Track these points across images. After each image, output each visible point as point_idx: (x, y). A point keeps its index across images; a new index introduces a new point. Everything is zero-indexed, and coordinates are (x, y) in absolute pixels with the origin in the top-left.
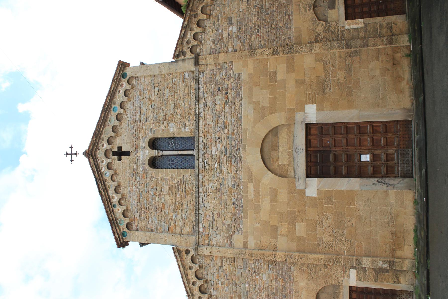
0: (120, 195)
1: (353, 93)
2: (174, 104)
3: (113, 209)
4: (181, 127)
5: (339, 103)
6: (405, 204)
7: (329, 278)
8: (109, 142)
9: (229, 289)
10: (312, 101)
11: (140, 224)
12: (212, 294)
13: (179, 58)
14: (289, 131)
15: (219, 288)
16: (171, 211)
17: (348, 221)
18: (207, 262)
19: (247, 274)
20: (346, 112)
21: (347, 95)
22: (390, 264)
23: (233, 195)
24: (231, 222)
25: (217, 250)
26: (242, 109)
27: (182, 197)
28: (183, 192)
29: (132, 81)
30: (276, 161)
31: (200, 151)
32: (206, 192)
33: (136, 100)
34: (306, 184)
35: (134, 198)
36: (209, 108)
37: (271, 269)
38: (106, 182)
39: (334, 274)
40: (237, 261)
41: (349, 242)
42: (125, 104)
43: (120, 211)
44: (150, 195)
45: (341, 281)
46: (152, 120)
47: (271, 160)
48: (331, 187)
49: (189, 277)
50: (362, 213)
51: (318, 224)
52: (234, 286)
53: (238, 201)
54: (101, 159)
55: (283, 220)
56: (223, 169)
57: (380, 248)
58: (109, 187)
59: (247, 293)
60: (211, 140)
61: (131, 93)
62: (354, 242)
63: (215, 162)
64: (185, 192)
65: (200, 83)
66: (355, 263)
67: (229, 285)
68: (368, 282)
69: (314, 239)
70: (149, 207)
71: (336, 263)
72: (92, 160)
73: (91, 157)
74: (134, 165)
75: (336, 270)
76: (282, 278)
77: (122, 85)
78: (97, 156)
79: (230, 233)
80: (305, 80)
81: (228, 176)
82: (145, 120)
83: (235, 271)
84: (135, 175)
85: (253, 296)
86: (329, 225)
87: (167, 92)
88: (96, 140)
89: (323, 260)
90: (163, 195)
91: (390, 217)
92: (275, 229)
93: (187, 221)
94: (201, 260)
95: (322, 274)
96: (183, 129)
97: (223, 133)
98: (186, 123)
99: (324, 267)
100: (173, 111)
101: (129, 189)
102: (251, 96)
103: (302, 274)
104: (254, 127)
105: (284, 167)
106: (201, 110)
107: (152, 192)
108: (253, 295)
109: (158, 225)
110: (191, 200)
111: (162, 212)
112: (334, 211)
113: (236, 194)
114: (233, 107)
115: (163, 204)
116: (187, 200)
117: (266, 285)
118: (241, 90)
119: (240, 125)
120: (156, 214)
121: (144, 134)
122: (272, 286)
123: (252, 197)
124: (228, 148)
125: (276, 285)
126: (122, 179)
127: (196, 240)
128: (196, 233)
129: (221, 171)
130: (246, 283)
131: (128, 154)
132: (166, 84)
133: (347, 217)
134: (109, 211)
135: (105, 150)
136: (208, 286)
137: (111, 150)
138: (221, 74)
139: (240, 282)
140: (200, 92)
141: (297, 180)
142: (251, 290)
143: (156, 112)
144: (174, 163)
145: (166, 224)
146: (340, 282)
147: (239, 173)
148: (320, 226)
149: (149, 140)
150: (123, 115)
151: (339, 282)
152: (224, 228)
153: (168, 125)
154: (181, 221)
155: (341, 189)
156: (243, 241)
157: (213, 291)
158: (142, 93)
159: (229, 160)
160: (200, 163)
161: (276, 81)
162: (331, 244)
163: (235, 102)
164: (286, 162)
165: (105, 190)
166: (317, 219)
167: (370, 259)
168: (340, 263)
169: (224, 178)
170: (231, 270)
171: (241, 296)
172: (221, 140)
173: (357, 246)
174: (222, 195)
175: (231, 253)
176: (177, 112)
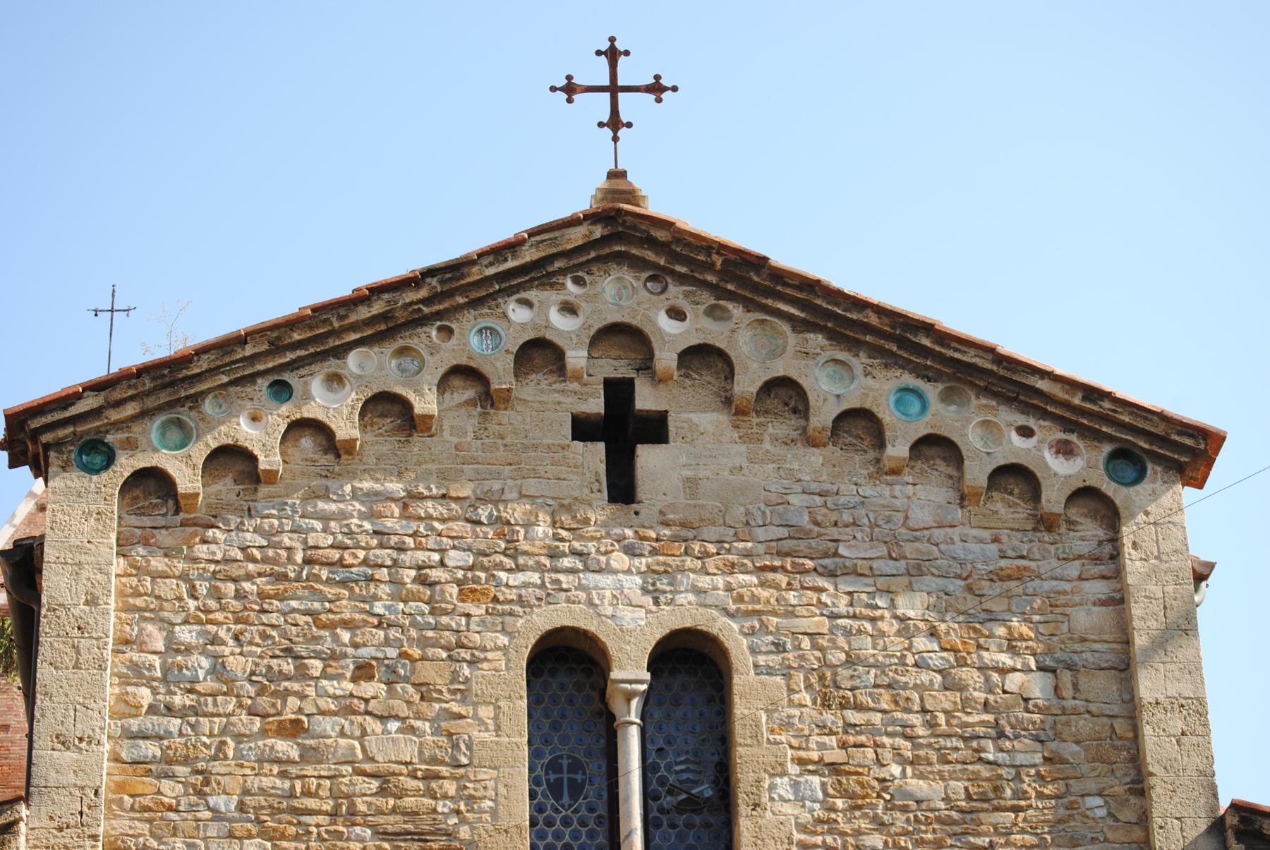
0: (356, 433)
3: (260, 381)
13: (1239, 841)
29: (1092, 515)
38: (434, 333)
42: (942, 466)
54: (589, 299)
58: (403, 352)
72: (576, 236)
73: (598, 232)
77: (1065, 450)
78: (607, 272)
87: (1020, 759)
88: (713, 264)
126: (455, 440)
134: (249, 351)
135: (647, 330)
137: (646, 365)
144: (566, 799)
149: (715, 631)
165: (383, 327)
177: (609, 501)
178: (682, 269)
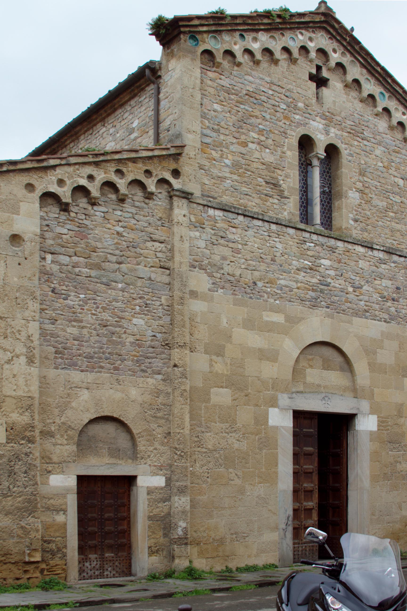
4: (355, 213)
5: (377, 463)
6: (262, 555)
7: (148, 441)
10: (381, 426)
12: (95, 208)
15: (109, 226)
18: (156, 210)
19: (142, 289)
20: (368, 472)
23: (267, 285)
26: (375, 320)
27: (258, 187)
28: (265, 191)
30: (309, 364)
31: (326, 239)
33: (388, 138)
34: (283, 409)
37: (154, 336)
40: (164, 272)
41: (206, 474)
45: (145, 462)
50: (248, 494)
51: (230, 426)
52: (118, 259)
53: (259, 292)
55: (234, 368)
56: (303, 274)
62: (207, 482)
64: (266, 195)
66: (181, 484)
67: (117, 249)
70: (239, 113)
71: (178, 453)
76: (141, 356)
79: (209, 267)
80: (402, 417)
82: (364, 148)
83: (145, 266)
86: (230, 442)
89: (182, 431)
90: (261, 149)
91: (244, 535)
92: (220, 353)
94: (160, 199)
95: (153, 428)
96: (351, 215)
99: (165, 433)
103: (149, 394)
105: (302, 376)
106: (376, 253)
107: (264, 128)
110: (254, 204)
111: (231, 137)
113: (269, 290)
114: (377, 307)
115: (245, 144)
116: (254, 195)
119: (356, 314)
120: (229, 123)
122: (124, 336)
123: (266, 318)
124: (329, 288)
125: (127, 344)
130: (123, 284)
133: (243, 472)
136: (111, 202)
139: (126, 272)
141: (290, 396)
142: (114, 293)
143: (373, 173)
148: (227, 429)
149: (338, 146)
150: (371, 108)
151: (142, 458)
152: (217, 258)
154: (220, 175)
156: (200, 290)
158: (397, 154)
159: (315, 288)
161: (404, 376)
163: (383, 311)
164: (309, 379)
166: (238, 425)
167: (188, 508)
168: (179, 459)
169: (290, 273)
170: (146, 257)
171: (99, 268)
174: (266, 265)
175: (181, 263)
176: (373, 211)
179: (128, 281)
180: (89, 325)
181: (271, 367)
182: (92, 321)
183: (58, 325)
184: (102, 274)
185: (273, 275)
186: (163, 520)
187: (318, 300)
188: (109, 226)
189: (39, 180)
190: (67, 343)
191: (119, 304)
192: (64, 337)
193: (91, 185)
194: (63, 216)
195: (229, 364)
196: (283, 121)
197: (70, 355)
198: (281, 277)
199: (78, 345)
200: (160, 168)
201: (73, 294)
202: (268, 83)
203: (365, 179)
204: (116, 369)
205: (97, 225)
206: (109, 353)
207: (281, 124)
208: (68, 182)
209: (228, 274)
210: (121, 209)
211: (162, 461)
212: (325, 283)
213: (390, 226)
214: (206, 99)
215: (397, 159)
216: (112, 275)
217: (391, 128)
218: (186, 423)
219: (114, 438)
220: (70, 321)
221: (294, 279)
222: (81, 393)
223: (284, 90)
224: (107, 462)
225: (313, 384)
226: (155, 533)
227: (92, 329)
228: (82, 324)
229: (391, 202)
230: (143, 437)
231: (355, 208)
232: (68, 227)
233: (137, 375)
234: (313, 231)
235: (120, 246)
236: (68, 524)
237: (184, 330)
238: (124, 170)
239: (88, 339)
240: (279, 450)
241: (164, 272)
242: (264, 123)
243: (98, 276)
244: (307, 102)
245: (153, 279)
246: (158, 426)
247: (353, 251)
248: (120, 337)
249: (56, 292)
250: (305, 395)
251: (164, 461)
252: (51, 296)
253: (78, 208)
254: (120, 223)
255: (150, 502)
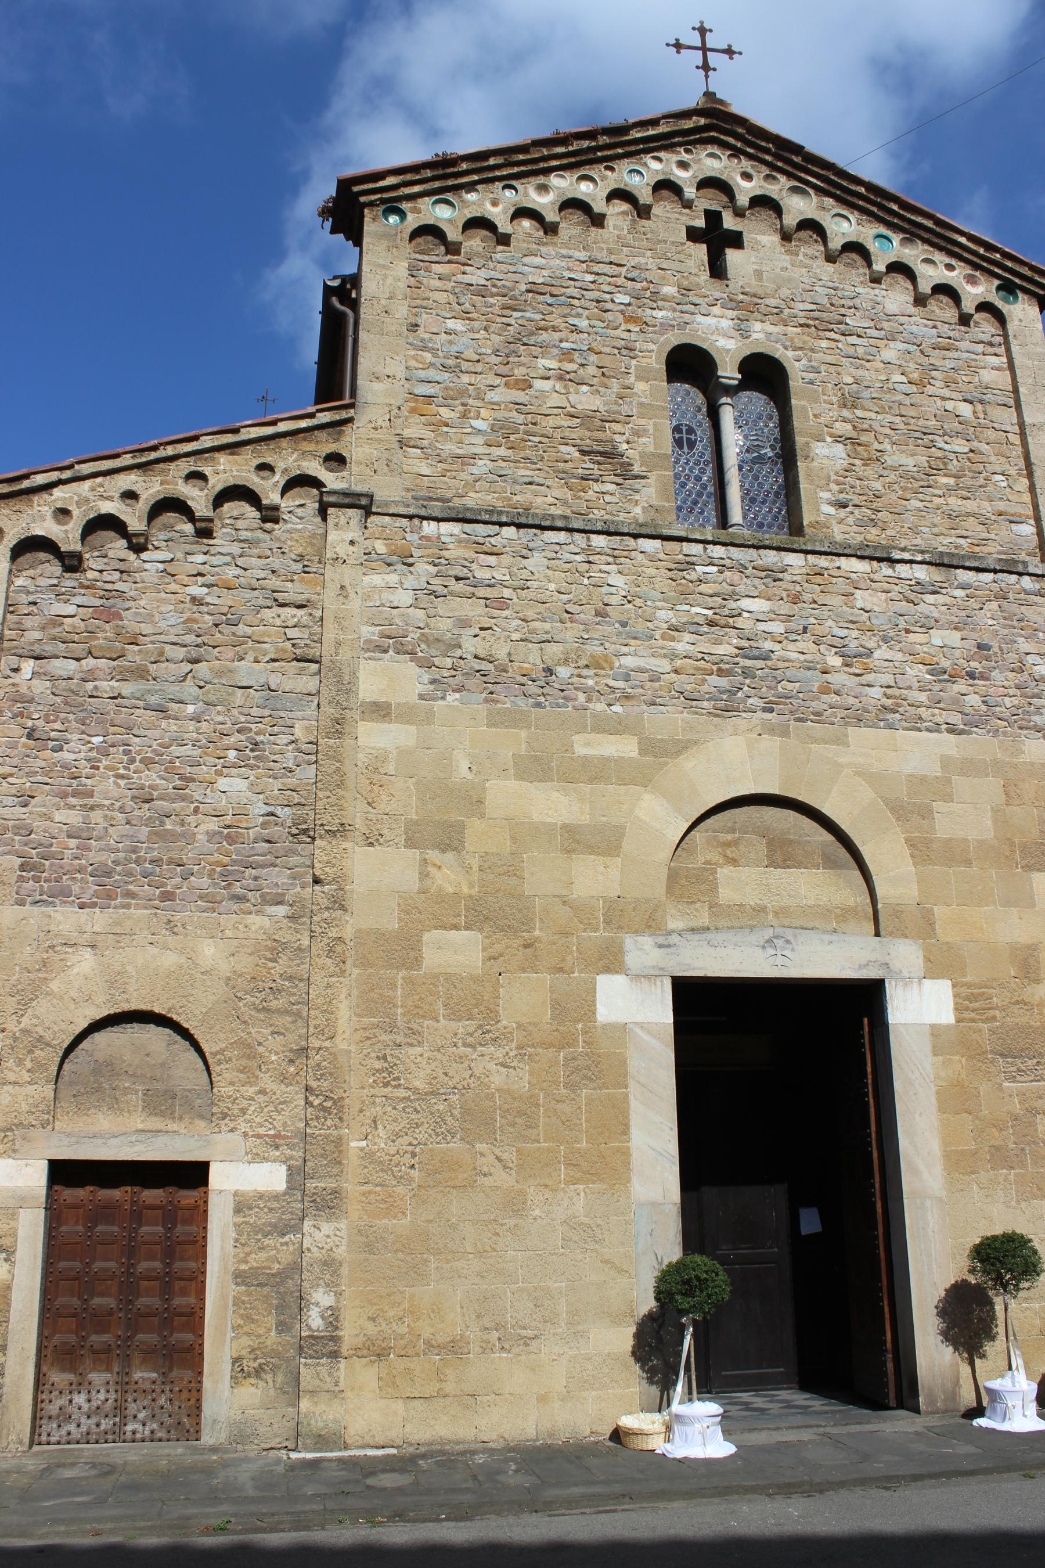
1: (1004, 1171)
2: (915, 469)
7: (241, 1071)
8: (762, 202)
9: (173, 630)
10: (967, 1009)
11: (437, 283)
12: (144, 556)
14: (845, 914)
16: (500, 415)
17: (499, 1154)
19: (246, 711)
20: (934, 1145)
21: (998, 1149)
22: (323, 1337)
23: (585, 672)
24: (469, 657)
25: (349, 587)
26: (919, 730)
27: (561, 465)
28: (580, 471)
30: (725, 856)
32: (589, 562)
33: (918, 325)
35: (545, 273)
36: (913, 602)
39: (260, 1092)
40: (303, 669)
41: (407, 1159)
43: (488, 206)
44: (563, 335)
46: (850, 380)
47: (729, 837)
48: (639, 1082)
49: (223, 460)
50: (537, 1212)
51: (480, 1026)
52: (189, 652)
53: (562, 691)
55: (491, 876)
56: (687, 637)
57: (389, 1295)
59: (159, 705)
60: (796, 599)
61: (943, 310)
62: (411, 1180)
63: (711, 608)
64: (583, 479)
65: (1000, 576)
66: (323, 1185)
67: (189, 631)
68: (232, 1243)
69: (416, 1007)
70: (509, 328)
71: (316, 1102)
73: (702, 121)
74: (676, 289)
75: (280, 1103)
76: (234, 862)
79: (423, 646)
81: (660, 656)
82: (851, 351)
84: (638, 286)
85: (142, 732)
86: (477, 1072)
87: (957, 449)
89: (327, 1044)
90: (565, 387)
91: (524, 1333)
93: (463, 476)
94: (301, 518)
95: (259, 1039)
96: (826, 495)
97: (827, 649)
98: (847, 509)
99: (291, 1050)
100: (889, 462)
101: (582, 255)
102: (969, 767)
104: (858, 773)
105: (703, 887)
106: (903, 570)
108: (146, 733)
109: (436, 356)
110: (550, 500)
112: (541, 1095)
113: (590, 682)
114: (923, 697)
116: (548, 482)
117: (195, 791)
118: (989, 732)
119: (858, 718)
120: (483, 350)
121: (796, 340)
122: (192, 819)
123: (580, 750)
124: (769, 663)
125: (199, 837)
127: (387, 504)
128: (417, 507)
129: (677, 630)
131: (717, 270)
132: (984, 447)
133: (518, 1150)
135: (731, 183)
136: (182, 540)
138: (1037, 657)
140: (971, 574)
141: (661, 940)
143: (880, 399)
144: (686, 449)
145: (446, 388)
146: (223, 1119)
147: (675, 701)
149: (777, 356)
151: (225, 1116)
152: (443, 626)
153: (838, 439)
154: (460, 452)
155: (632, 1123)
157: (162, 559)
160: (705, 549)
161: (1028, 868)
162: (393, 1083)
163: (941, 705)
164: (726, 894)
166: (505, 1022)
168: (317, 1118)
169: (651, 637)
171: (142, 678)
172: (799, 638)
173: (390, 1196)
174: (582, 627)
176: (888, 480)
177: (711, 277)
178: (751, 151)
179: (212, 698)
180: (107, 802)
181: (601, 868)
182: (115, 792)
183: (35, 806)
184: (149, 687)
185: (601, 648)
186: (277, 1284)
187: (739, 695)
188: (174, 587)
189: (14, 517)
190: (51, 845)
191: (187, 750)
192: (45, 832)
193: (129, 509)
194: (70, 581)
195: (475, 868)
196: (623, 327)
197: (56, 872)
198: (625, 649)
199: (78, 848)
200: (295, 456)
201: (75, 737)
202: (583, 262)
203: (859, 413)
204: (168, 896)
205: (145, 588)
206: (151, 862)
207: (618, 333)
208: (76, 512)
209: (476, 657)
210: (205, 549)
211: (278, 1125)
212: (756, 652)
213: (945, 507)
214: (427, 313)
215: (947, 361)
216: (173, 690)
217: (920, 301)
218: (340, 1022)
219: (163, 1065)
220: (64, 796)
221: (665, 651)
222: (75, 959)
223: (624, 269)
224: (140, 1126)
225: (741, 905)
226: (253, 1321)
227: (113, 810)
228: (90, 801)
229: (940, 454)
230: (228, 1060)
231: (833, 477)
232: (78, 600)
233: (222, 910)
234: (711, 539)
235: (196, 626)
236: (14, 1287)
237: (341, 792)
238: (207, 471)
239: (102, 833)
240: (633, 1088)
241: (303, 669)
242: (574, 337)
243: (138, 695)
244: (685, 283)
245: (273, 688)
246: (273, 1033)
247: (835, 573)
248: (182, 823)
249: (37, 736)
250: (709, 936)
251: (285, 1124)
252: (25, 746)
253: (105, 560)
254: (199, 578)
255: (240, 1233)
